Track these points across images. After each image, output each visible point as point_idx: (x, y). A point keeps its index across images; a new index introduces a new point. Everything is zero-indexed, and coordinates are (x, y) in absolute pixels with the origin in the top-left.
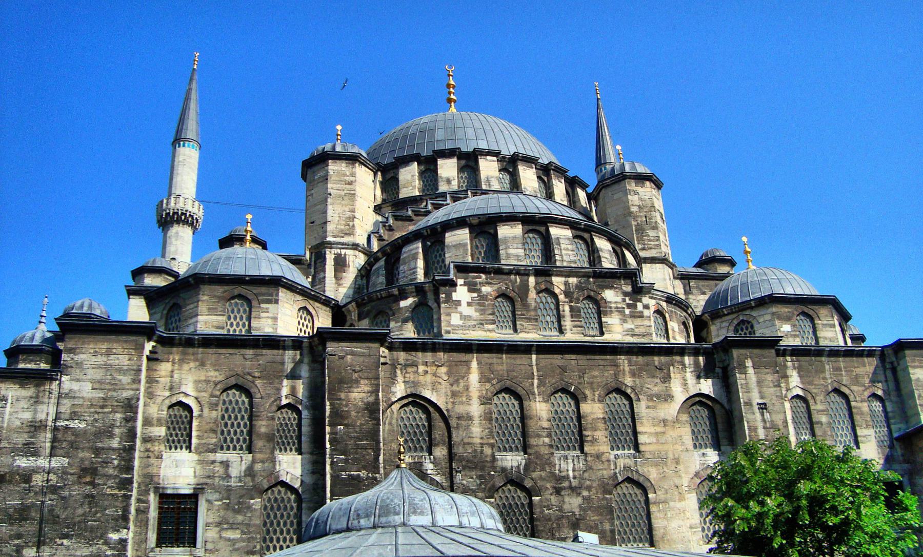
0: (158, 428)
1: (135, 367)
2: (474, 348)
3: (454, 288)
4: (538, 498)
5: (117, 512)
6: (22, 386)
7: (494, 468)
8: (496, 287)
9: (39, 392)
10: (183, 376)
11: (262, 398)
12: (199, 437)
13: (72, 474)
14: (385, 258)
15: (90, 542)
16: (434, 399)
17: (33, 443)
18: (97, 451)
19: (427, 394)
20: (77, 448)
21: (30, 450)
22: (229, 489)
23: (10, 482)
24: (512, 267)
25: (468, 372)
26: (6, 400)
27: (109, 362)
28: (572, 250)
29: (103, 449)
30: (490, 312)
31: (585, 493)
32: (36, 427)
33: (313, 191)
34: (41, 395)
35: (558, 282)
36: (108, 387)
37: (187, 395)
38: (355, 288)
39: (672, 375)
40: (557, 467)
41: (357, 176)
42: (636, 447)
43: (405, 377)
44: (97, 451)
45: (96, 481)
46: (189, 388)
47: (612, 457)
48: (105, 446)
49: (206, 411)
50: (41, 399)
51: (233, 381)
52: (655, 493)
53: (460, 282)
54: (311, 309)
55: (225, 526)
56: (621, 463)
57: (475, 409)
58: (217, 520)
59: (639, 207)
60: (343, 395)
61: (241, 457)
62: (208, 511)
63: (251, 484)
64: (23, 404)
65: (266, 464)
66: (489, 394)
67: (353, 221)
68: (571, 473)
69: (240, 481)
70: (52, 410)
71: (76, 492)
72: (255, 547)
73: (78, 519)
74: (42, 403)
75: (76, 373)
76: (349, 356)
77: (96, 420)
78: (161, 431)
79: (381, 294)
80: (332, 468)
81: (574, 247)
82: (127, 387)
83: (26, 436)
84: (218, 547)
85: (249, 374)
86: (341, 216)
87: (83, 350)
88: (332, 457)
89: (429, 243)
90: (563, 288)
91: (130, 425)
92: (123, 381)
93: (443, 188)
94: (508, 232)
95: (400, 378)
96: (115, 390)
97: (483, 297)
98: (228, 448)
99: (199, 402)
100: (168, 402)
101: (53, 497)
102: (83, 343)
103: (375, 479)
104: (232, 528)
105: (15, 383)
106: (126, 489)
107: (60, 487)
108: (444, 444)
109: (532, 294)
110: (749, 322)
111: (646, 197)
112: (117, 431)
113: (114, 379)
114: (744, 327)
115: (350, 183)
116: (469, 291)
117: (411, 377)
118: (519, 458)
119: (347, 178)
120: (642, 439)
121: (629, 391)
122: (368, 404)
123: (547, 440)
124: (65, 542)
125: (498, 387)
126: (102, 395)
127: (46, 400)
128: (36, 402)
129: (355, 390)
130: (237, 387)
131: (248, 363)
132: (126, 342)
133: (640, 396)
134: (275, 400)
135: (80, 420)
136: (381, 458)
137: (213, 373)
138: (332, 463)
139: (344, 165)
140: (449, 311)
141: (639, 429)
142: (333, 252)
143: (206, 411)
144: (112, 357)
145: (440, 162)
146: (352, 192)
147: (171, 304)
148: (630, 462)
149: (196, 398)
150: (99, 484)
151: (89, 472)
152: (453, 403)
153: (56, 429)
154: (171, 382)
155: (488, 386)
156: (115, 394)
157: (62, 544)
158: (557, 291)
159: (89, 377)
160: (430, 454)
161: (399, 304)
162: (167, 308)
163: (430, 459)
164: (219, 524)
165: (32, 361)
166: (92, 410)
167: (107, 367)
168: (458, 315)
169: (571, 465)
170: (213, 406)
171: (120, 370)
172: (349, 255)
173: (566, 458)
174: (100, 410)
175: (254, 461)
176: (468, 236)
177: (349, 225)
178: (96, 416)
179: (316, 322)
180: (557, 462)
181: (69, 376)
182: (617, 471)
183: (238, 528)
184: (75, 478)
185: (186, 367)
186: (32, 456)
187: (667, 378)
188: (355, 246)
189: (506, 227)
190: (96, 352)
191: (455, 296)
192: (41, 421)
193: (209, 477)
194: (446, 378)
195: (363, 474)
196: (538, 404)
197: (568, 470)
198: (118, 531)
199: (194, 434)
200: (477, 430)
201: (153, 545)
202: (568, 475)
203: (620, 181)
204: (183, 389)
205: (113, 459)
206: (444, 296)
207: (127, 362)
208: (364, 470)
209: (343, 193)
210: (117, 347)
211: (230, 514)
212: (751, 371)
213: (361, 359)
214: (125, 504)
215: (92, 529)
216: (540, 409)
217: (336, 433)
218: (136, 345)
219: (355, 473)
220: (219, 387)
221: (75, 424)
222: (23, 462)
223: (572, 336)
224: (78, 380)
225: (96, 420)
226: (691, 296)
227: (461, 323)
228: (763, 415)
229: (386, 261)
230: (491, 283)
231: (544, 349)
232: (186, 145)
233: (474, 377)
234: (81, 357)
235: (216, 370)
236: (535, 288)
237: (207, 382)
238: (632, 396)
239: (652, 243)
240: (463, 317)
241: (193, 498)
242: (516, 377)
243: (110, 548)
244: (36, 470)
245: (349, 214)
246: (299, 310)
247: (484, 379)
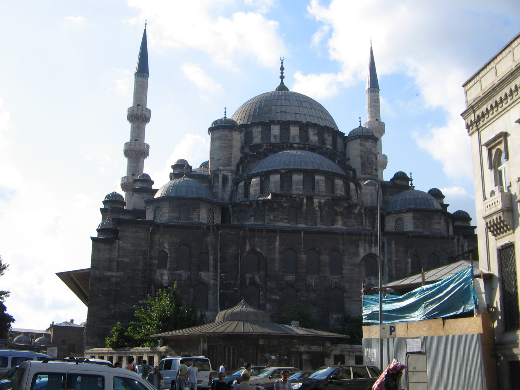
2: (278, 231)
4: (299, 293)
5: (142, 293)
8: (289, 204)
12: (170, 264)
14: (244, 181)
19: (259, 250)
21: (110, 269)
24: (296, 196)
25: (275, 241)
28: (324, 186)
31: (318, 292)
32: (111, 260)
33: (213, 143)
37: (165, 248)
38: (231, 191)
39: (360, 245)
40: (308, 281)
41: (234, 136)
42: (341, 273)
43: (250, 243)
46: (166, 246)
47: (331, 278)
52: (347, 293)
54: (213, 209)
56: (334, 281)
57: (277, 256)
59: (365, 152)
61: (186, 273)
67: (231, 159)
68: (313, 284)
70: (116, 254)
76: (228, 235)
79: (242, 203)
81: (325, 185)
86: (226, 156)
88: (220, 274)
89: (263, 179)
90: (318, 204)
93: (272, 140)
94: (297, 178)
95: (248, 244)
99: (170, 251)
103: (236, 283)
109: (304, 207)
110: (402, 219)
111: (368, 147)
112: (141, 263)
114: (400, 221)
115: (230, 140)
118: (293, 277)
119: (229, 138)
120: (345, 271)
121: (341, 251)
123: (305, 270)
124: (124, 303)
133: (346, 254)
136: (239, 275)
138: (221, 277)
139: (227, 131)
141: (344, 267)
142: (222, 174)
145: (272, 127)
146: (231, 145)
147: (156, 206)
148: (338, 280)
153: (118, 262)
158: (315, 206)
162: (155, 207)
163: (258, 276)
169: (314, 281)
172: (229, 176)
173: (312, 278)
176: (279, 178)
177: (229, 161)
179: (215, 214)
180: (308, 279)
181: (122, 241)
182: (332, 284)
186: (110, 271)
187: (358, 247)
188: (232, 171)
189: (296, 175)
194: (266, 243)
195: (232, 282)
196: (302, 255)
197: (312, 283)
198: (141, 300)
199: (168, 263)
200: (277, 265)
202: (312, 285)
203: (357, 139)
205: (139, 273)
206: (267, 207)
208: (232, 280)
209: (226, 145)
212: (393, 246)
216: (303, 257)
221: (125, 259)
223: (321, 226)
226: (385, 197)
228: (396, 264)
229: (245, 183)
230: (287, 202)
231: (307, 232)
232: (142, 76)
233: (277, 244)
236: (306, 204)
238: (342, 253)
239: (369, 171)
244: (113, 276)
245: (229, 156)
246: (208, 210)
247: (281, 245)
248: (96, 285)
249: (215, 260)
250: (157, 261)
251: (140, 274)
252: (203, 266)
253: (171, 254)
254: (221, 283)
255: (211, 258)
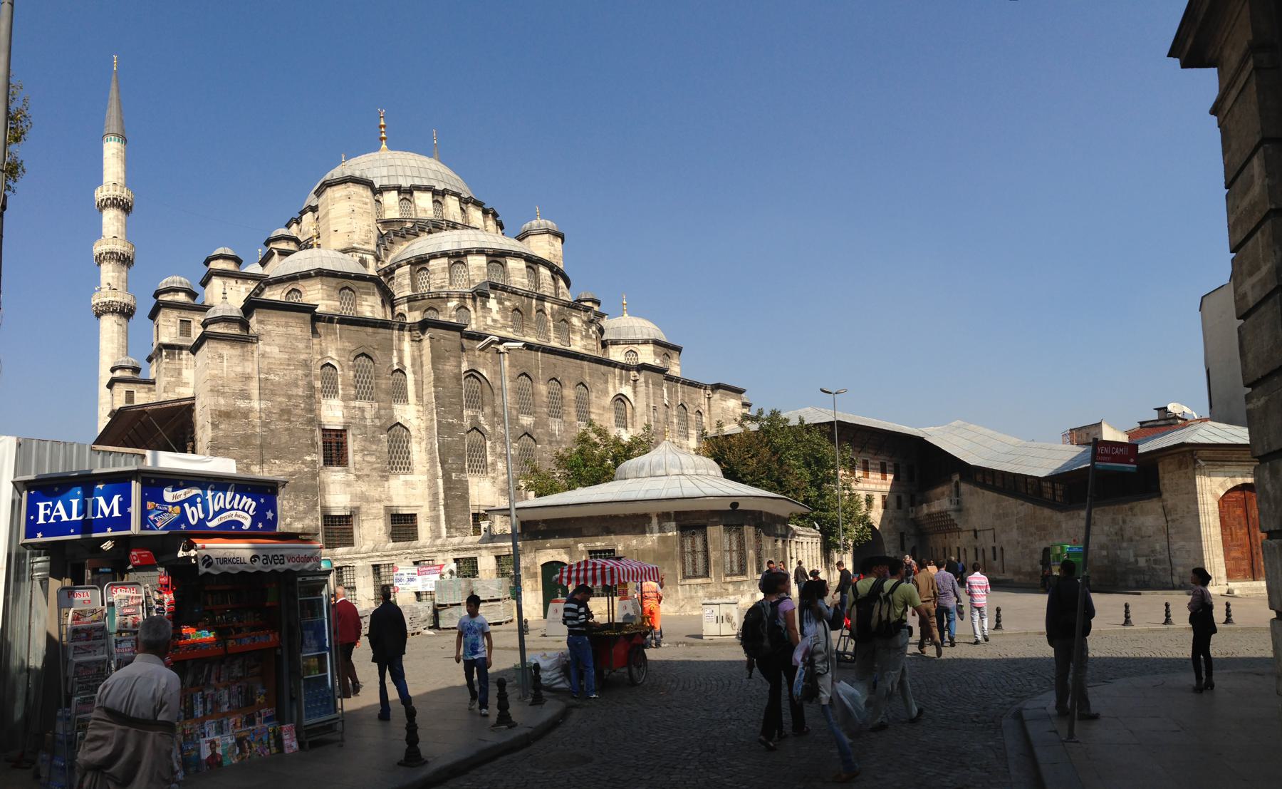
0: (316, 382)
1: (306, 337)
3: (487, 299)
6: (232, 347)
7: (518, 424)
9: (244, 352)
10: (329, 345)
11: (380, 364)
12: (342, 389)
13: (274, 413)
15: (292, 462)
16: (485, 374)
17: (246, 390)
18: (290, 397)
19: (481, 371)
20: (276, 395)
22: (365, 426)
23: (234, 418)
26: (223, 357)
27: (288, 332)
29: (293, 395)
30: (509, 319)
34: (246, 354)
35: (548, 305)
36: (290, 350)
37: (332, 359)
44: (290, 397)
45: (292, 419)
48: (294, 393)
49: (346, 370)
50: (246, 358)
51: (360, 351)
53: (492, 296)
55: (366, 453)
57: (507, 384)
58: (361, 448)
60: (440, 367)
62: (354, 441)
63: (379, 424)
64: (235, 360)
65: (387, 411)
66: (516, 376)
69: (373, 422)
71: (281, 425)
72: (386, 467)
73: (283, 446)
74: (248, 360)
75: (266, 339)
77: (285, 375)
78: (318, 384)
80: (437, 416)
82: (303, 351)
83: (240, 384)
84: (363, 467)
85: (371, 346)
87: (270, 322)
91: (308, 379)
92: (300, 346)
94: (514, 265)
96: (294, 353)
97: (505, 309)
98: (361, 399)
99: (341, 364)
100: (320, 363)
101: (264, 429)
102: (269, 317)
103: (462, 425)
104: (370, 454)
105: (227, 345)
106: (312, 425)
107: (268, 422)
108: (489, 405)
112: (300, 383)
113: (293, 345)
116: (498, 303)
117: (471, 358)
122: (455, 374)
124: (277, 461)
125: (521, 371)
126: (287, 357)
127: (251, 359)
128: (243, 359)
129: (448, 364)
130: (363, 354)
131: (370, 338)
132: (297, 318)
134: (390, 366)
135: (275, 375)
137: (347, 344)
140: (486, 315)
143: (346, 370)
144: (289, 329)
149: (339, 361)
150: (293, 421)
151: (286, 413)
152: (495, 378)
154: (321, 348)
155: (515, 370)
156: (295, 356)
157: (275, 463)
159: (277, 342)
160: (483, 410)
161: (446, 304)
164: (362, 451)
165: (232, 328)
166: (282, 367)
167: (288, 336)
168: (490, 319)
170: (350, 368)
171: (296, 339)
174: (286, 367)
175: (379, 409)
178: (285, 372)
183: (373, 454)
184: (277, 416)
185: (329, 338)
186: (246, 399)
190: (278, 324)
191: (488, 305)
192: (248, 374)
193: (352, 418)
195: (455, 421)
199: (340, 387)
201: (322, 465)
204: (329, 354)
207: (301, 333)
210: (292, 322)
211: (368, 444)
213: (450, 343)
214: (312, 436)
215: (293, 453)
217: (438, 392)
218: (304, 320)
219: (451, 420)
220: (352, 354)
221: (272, 377)
222: (242, 404)
224: (269, 345)
225: (285, 375)
227: (492, 324)
234: (269, 327)
235: (349, 342)
237: (344, 350)
240: (494, 321)
241: (345, 430)
242: (529, 366)
243: (307, 467)
247: (512, 365)
248: (222, 426)
249: (419, 384)
250: (320, 382)
251: (302, 405)
252: (399, 394)
253: (343, 370)
254: (439, 422)
255: (410, 378)
